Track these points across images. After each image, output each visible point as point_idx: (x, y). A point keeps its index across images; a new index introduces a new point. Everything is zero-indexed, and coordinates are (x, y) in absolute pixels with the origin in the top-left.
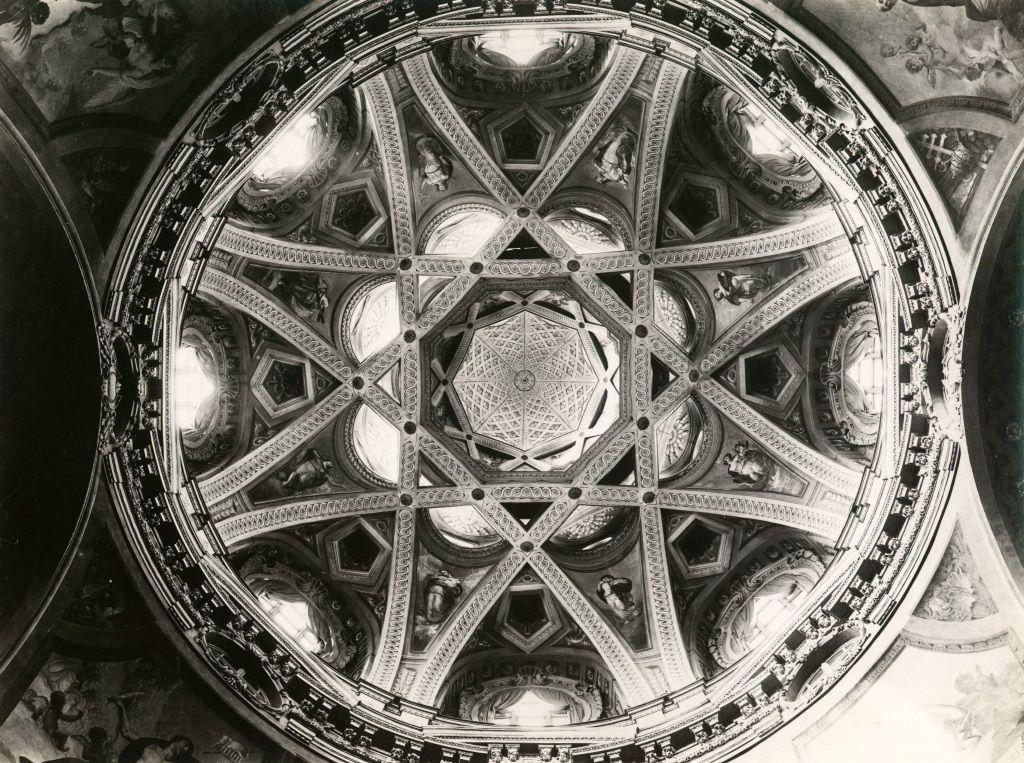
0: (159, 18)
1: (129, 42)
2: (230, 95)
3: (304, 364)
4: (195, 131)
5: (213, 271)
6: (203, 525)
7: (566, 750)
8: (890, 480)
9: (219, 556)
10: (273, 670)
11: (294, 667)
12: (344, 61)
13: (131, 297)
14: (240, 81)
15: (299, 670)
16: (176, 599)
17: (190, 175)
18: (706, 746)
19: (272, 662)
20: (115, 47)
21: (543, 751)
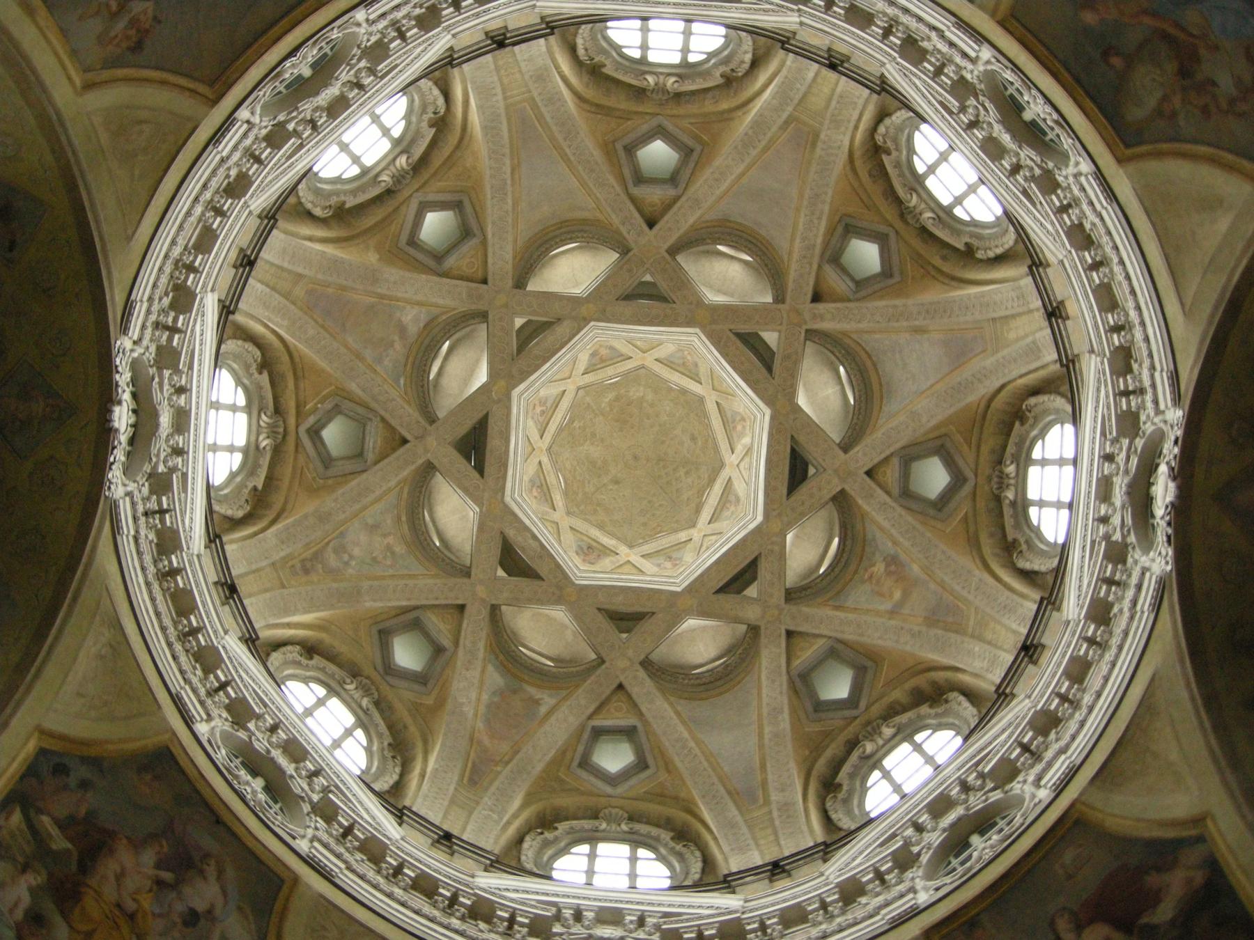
0: (158, 866)
1: (179, 907)
2: (254, 792)
3: (593, 728)
4: (294, 838)
7: (1108, 443)
8: (803, 19)
10: (976, 802)
11: (975, 774)
12: (224, 647)
14: (236, 777)
15: (980, 768)
16: (878, 913)
17: (347, 849)
18: (1117, 269)
19: (966, 801)
20: (186, 924)
21: (1106, 472)
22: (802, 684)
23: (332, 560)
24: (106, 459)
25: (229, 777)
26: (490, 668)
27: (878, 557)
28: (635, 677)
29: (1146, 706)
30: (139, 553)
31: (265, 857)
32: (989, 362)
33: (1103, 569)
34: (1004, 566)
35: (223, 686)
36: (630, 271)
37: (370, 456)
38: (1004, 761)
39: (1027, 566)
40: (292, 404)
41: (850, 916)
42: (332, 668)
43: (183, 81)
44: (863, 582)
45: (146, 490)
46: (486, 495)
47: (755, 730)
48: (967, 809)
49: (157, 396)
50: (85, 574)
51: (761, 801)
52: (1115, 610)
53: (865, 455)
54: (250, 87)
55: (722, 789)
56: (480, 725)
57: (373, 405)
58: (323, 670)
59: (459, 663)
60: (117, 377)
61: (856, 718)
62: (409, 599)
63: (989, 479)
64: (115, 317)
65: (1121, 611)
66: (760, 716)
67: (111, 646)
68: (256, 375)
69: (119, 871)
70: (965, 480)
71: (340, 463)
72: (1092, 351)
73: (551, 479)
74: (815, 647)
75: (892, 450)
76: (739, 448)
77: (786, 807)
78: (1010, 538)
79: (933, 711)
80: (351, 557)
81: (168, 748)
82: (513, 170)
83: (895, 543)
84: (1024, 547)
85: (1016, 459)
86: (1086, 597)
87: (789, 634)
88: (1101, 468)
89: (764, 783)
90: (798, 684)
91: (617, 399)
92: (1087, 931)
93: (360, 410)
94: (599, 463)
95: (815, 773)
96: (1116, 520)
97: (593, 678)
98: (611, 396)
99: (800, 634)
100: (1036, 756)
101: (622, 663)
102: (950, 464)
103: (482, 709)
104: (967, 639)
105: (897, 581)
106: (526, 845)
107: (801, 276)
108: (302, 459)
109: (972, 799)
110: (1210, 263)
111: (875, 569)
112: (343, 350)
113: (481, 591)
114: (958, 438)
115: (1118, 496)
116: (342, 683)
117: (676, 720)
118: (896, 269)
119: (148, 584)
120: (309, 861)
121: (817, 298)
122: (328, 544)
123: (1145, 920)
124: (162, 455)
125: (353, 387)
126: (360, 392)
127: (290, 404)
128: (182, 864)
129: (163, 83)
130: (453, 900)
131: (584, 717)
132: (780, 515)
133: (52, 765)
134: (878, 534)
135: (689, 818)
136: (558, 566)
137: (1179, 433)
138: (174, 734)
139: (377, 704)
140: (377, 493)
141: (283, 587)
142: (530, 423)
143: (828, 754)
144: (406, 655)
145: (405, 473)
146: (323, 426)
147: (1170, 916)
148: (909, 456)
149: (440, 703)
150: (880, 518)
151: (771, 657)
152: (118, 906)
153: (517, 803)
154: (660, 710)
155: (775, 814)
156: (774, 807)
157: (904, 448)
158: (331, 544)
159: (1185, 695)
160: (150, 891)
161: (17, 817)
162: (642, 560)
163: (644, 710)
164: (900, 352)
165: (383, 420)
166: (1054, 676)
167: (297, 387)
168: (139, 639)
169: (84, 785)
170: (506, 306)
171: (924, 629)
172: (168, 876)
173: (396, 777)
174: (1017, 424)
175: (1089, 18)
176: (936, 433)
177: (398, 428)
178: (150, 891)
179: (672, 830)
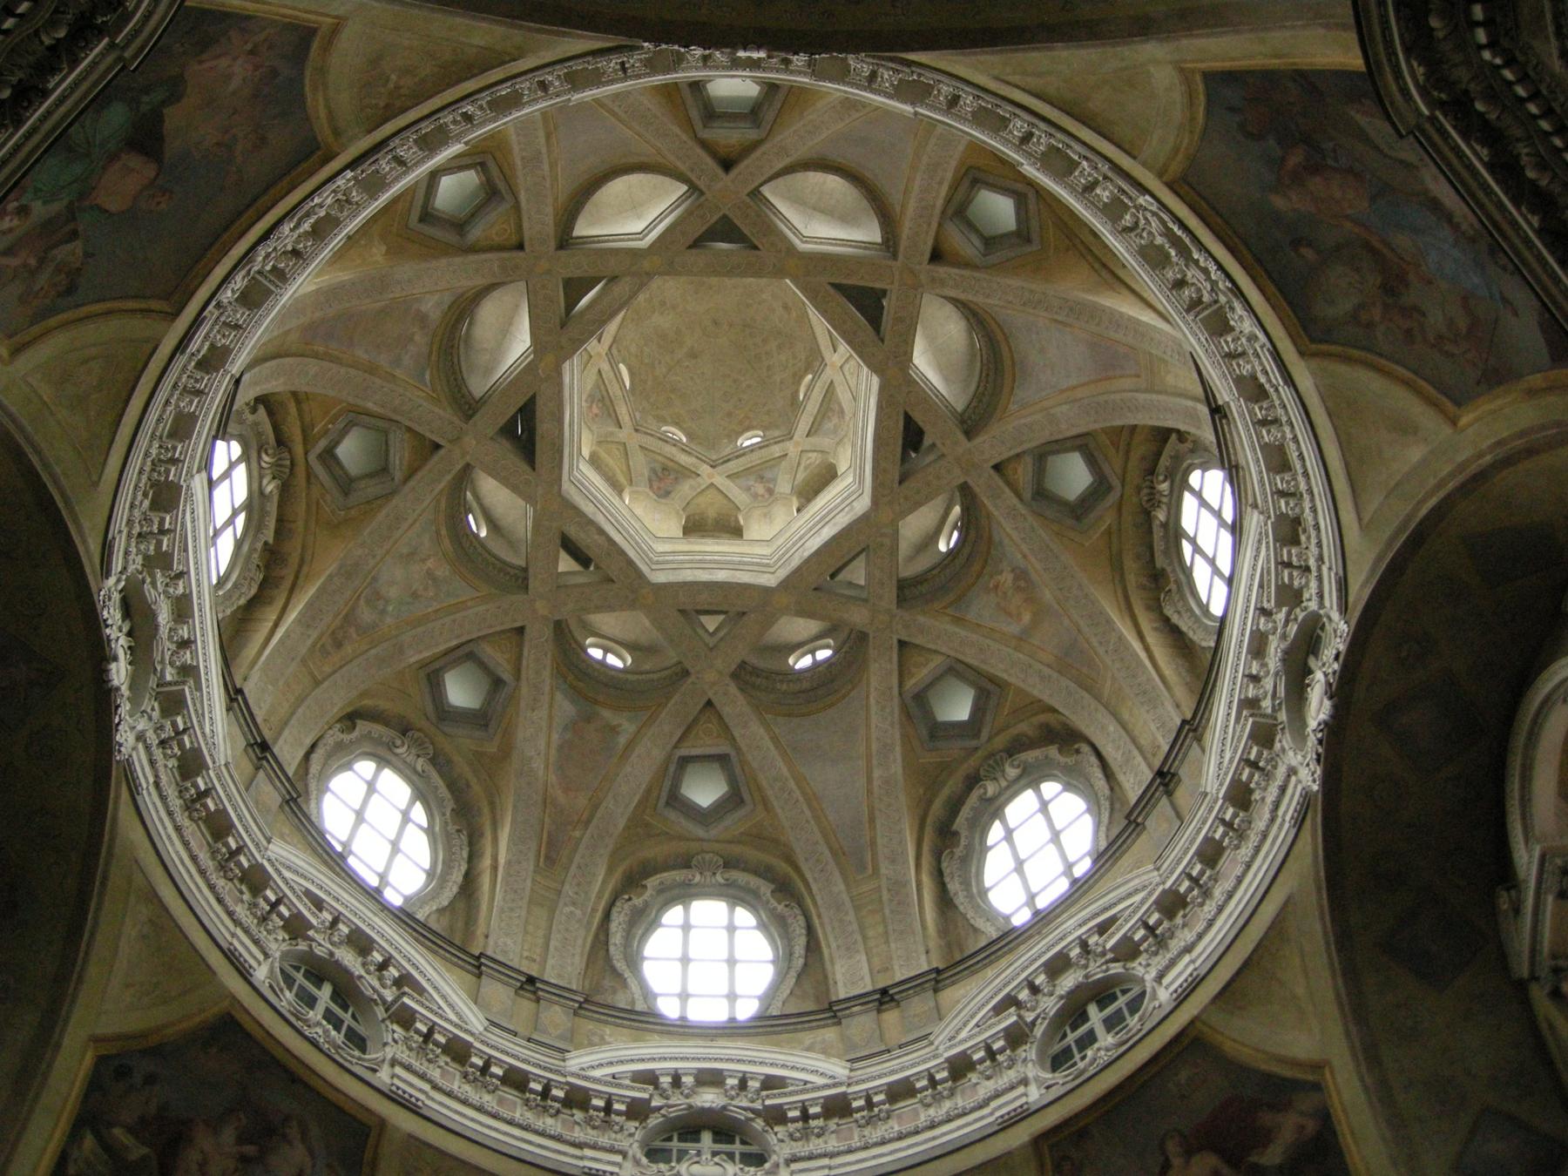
0: (241, 1140)
5: (551, 962)
6: (892, 1000)
9: (938, 982)
10: (1096, 970)
13: (590, 1135)
14: (305, 1021)
19: (1086, 967)
22: (917, 707)
23: (366, 615)
24: (111, 721)
25: (299, 1024)
26: (559, 696)
29: (1277, 927)
30: (163, 798)
31: (347, 1107)
32: (1141, 397)
33: (1247, 749)
34: (1148, 608)
35: (274, 906)
37: (398, 475)
38: (1127, 939)
39: (1175, 619)
41: (960, 1102)
42: (378, 729)
43: (131, 304)
45: (156, 714)
47: (859, 769)
48: (1086, 976)
50: (110, 854)
51: (870, 871)
54: (218, 280)
55: (827, 852)
56: (553, 778)
58: (368, 737)
59: (523, 704)
60: (108, 631)
61: (977, 749)
62: (458, 637)
64: (92, 566)
65: (1263, 799)
66: (868, 747)
68: (250, 418)
70: (1110, 488)
71: (363, 484)
72: (1255, 506)
73: (614, 389)
74: (932, 665)
77: (898, 886)
78: (1158, 565)
79: (1062, 759)
80: (387, 602)
81: (229, 1014)
82: (548, 136)
83: (1025, 556)
84: (1173, 586)
85: (1170, 476)
86: (1226, 774)
87: (902, 644)
88: (1256, 622)
89: (873, 843)
92: (1196, 1159)
93: (380, 423)
95: (929, 821)
96: (1268, 683)
97: (677, 697)
99: (917, 646)
100: (1162, 943)
101: (710, 676)
102: (1092, 462)
103: (553, 752)
104: (1101, 708)
105: (1025, 601)
106: (613, 926)
109: (1092, 964)
110: (1397, 485)
111: (1002, 578)
112: (353, 372)
113: (541, 607)
115: (1273, 660)
116: (391, 746)
117: (774, 752)
118: (1035, 236)
119: (178, 829)
120: (392, 1097)
121: (937, 256)
123: (1254, 1159)
124: (167, 655)
125: (370, 405)
128: (264, 1134)
129: (109, 313)
130: (545, 1093)
131: (669, 747)
133: (115, 1068)
134: (1006, 541)
135: (790, 870)
136: (630, 562)
137: (1342, 647)
139: (433, 761)
140: (410, 521)
141: (317, 683)
143: (945, 792)
144: (460, 692)
146: (337, 443)
147: (1277, 1161)
148: (1043, 455)
149: (506, 753)
150: (1008, 526)
151: (880, 672)
153: (601, 873)
154: (755, 736)
155: (885, 896)
156: (884, 882)
159: (1318, 927)
161: (89, 1141)
162: (728, 482)
163: (736, 735)
165: (409, 429)
166: (1185, 853)
167: (300, 410)
168: (180, 901)
169: (150, 1079)
171: (1055, 675)
173: (464, 867)
174: (1174, 436)
175: (1279, 202)
177: (428, 435)
179: (772, 881)
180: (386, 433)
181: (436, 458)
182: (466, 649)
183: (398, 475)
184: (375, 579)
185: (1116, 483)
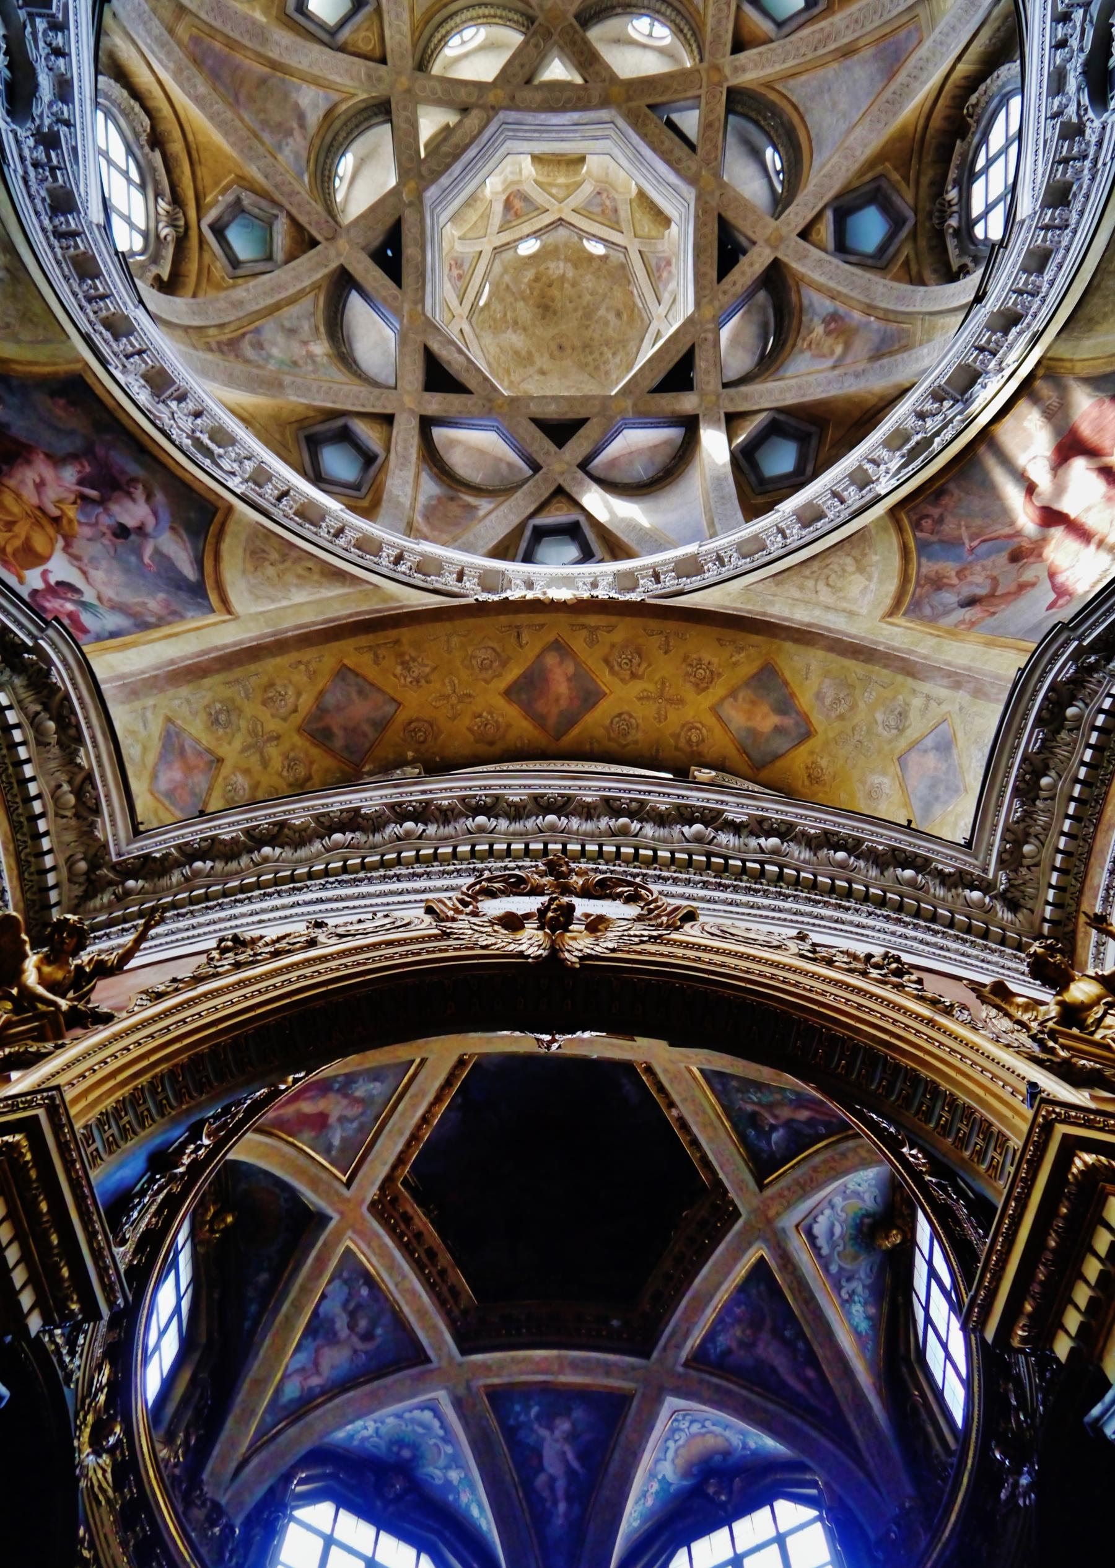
0: (81, 482)
1: (105, 520)
3: (535, 528)
27: (817, 321)
28: (574, 479)
31: (196, 486)
36: (537, 46)
40: (190, 194)
44: (802, 351)
46: (406, 307)
49: (33, 54)
52: (1075, 188)
53: (798, 214)
57: (278, 197)
63: (930, 215)
67: (8, 270)
69: (38, 480)
75: (825, 200)
76: (666, 297)
80: (270, 356)
85: (957, 183)
90: (742, 461)
91: (537, 279)
94: (524, 353)
98: (530, 274)
101: (557, 467)
102: (888, 210)
107: (719, 22)
108: (207, 257)
111: (814, 335)
112: (239, 124)
113: (409, 401)
114: (896, 176)
121: (738, 46)
122: (244, 335)
125: (253, 171)
126: (259, 177)
127: (190, 194)
128: (106, 485)
132: (711, 301)
138: (87, 364)
142: (448, 286)
145: (319, 275)
146: (227, 226)
148: (844, 209)
152: (40, 508)
157: (837, 197)
158: (248, 337)
160: (74, 503)
164: (829, 89)
170: (409, 91)
172: (93, 493)
176: (869, 176)
177: (307, 226)
178: (74, 503)
180: (271, 226)
181: (313, 252)
182: (339, 422)
183: (279, 255)
184: (257, 331)
185: (909, 214)
